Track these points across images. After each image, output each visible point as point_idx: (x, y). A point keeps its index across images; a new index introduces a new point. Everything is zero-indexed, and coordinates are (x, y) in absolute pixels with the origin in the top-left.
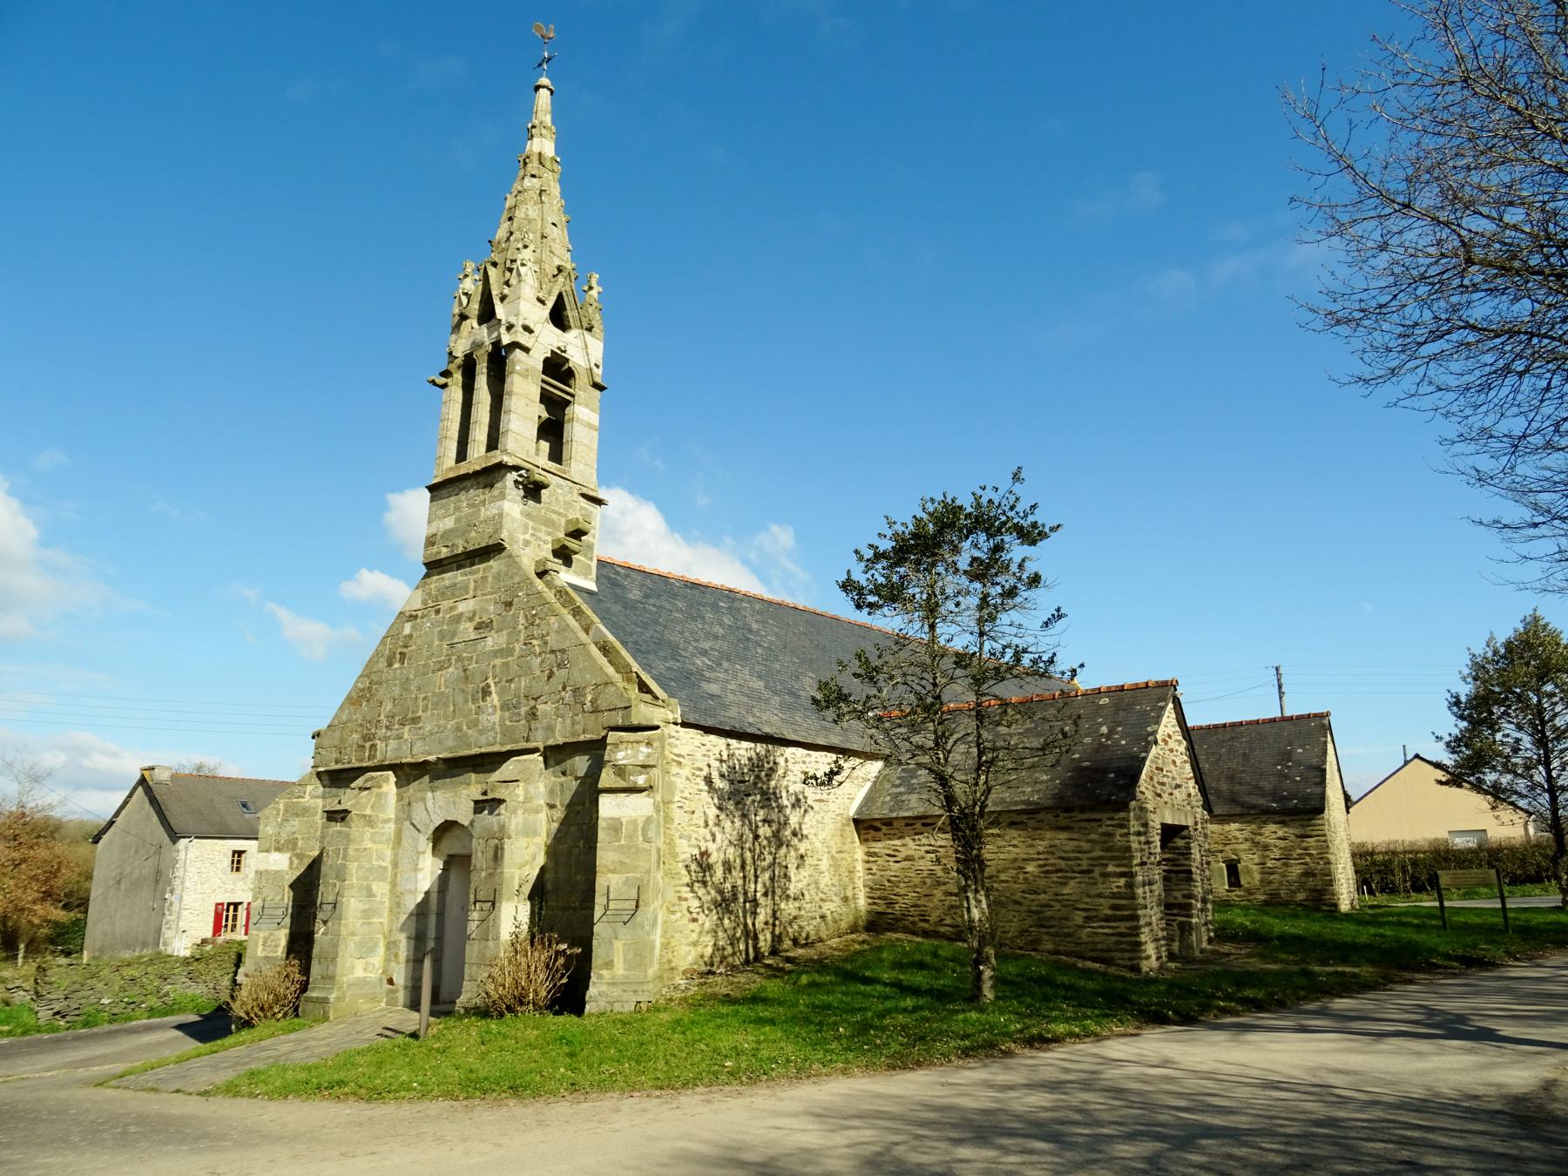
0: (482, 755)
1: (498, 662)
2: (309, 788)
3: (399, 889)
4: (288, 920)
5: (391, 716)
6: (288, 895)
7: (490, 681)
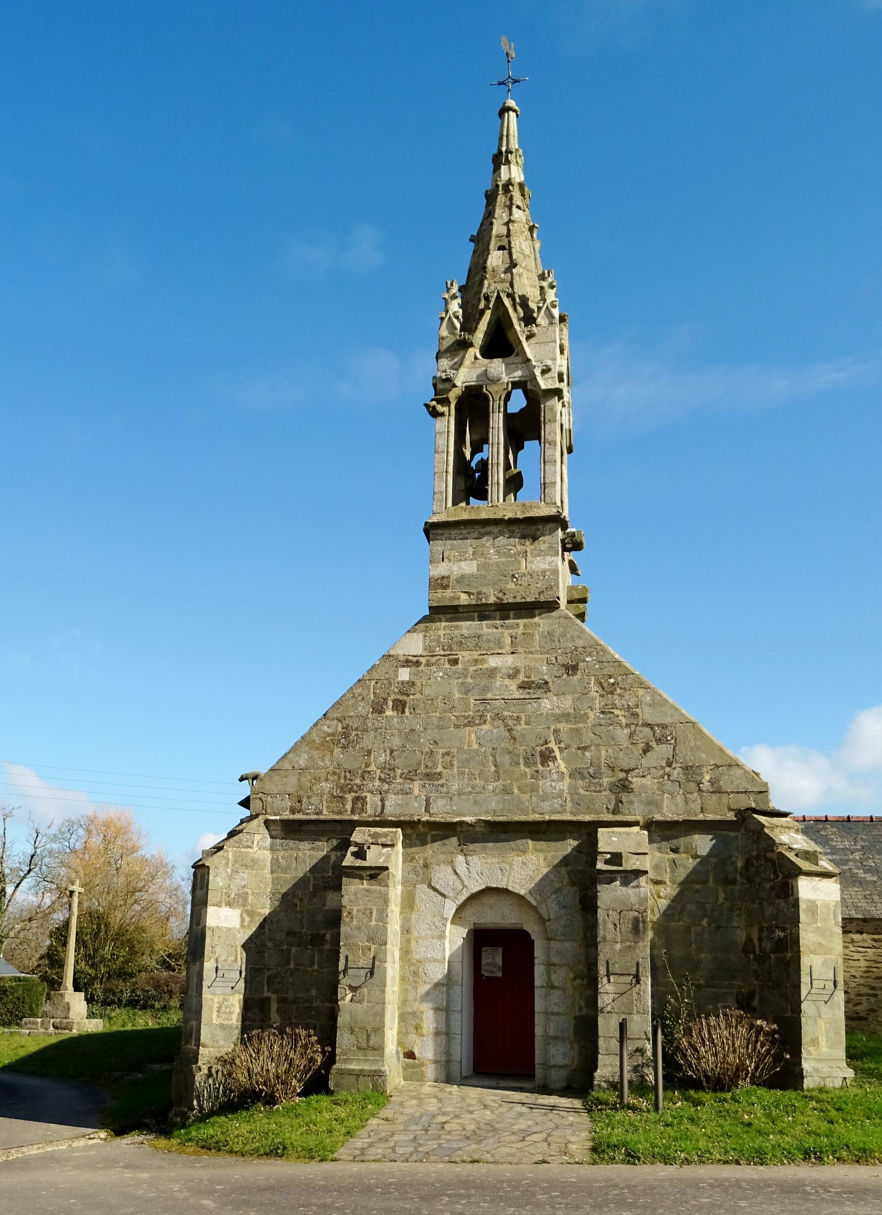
0: (550, 822)
1: (563, 726)
2: (257, 837)
3: (415, 956)
4: (241, 985)
5: (389, 770)
6: (242, 955)
7: (552, 745)
